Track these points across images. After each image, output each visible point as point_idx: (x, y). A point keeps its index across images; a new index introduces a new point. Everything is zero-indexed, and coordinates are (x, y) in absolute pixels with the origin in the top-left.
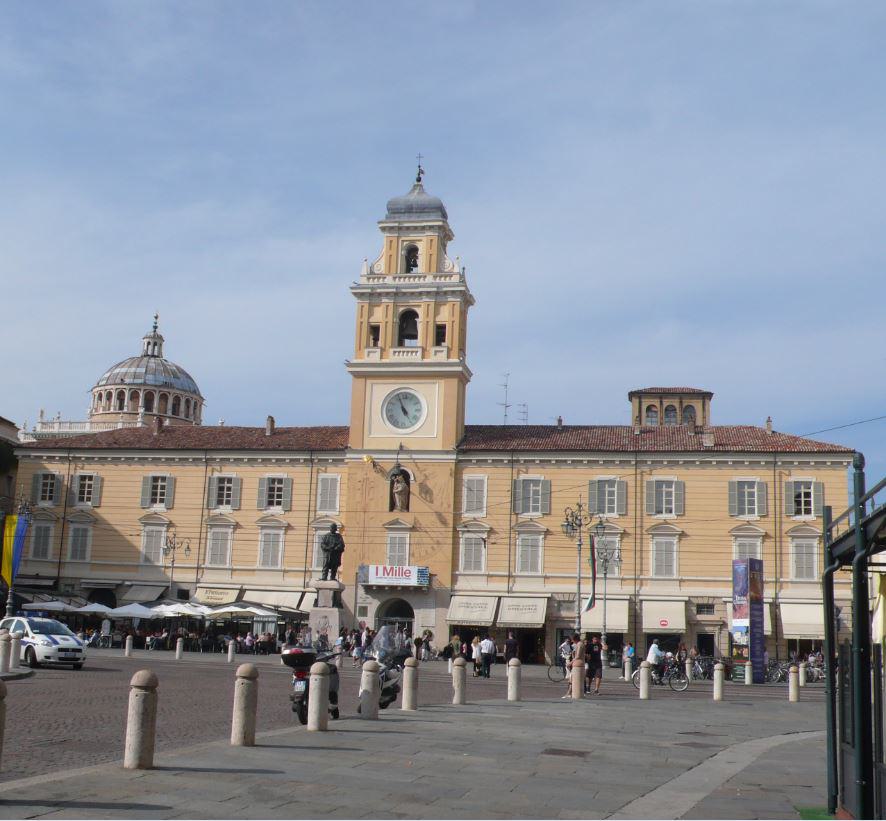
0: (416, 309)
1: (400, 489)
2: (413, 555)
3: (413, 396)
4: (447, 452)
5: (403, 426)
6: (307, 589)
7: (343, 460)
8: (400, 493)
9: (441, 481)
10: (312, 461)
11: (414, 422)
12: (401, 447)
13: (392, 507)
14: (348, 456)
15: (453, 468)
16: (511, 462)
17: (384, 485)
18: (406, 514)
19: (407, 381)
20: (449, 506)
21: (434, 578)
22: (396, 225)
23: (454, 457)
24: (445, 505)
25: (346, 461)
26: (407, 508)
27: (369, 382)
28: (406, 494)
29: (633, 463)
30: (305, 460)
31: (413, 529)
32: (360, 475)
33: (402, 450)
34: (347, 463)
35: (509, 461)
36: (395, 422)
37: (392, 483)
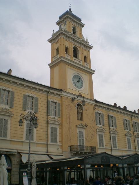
0: (78, 48)
6: (48, 154)
7: (59, 95)
10: (48, 92)
14: (63, 93)
16: (108, 109)
22: (72, 18)
23: (94, 103)
25: (61, 95)
27: (67, 66)
29: (131, 115)
30: (45, 91)
33: (80, 96)
34: (62, 97)
35: (107, 108)
37: (77, 109)
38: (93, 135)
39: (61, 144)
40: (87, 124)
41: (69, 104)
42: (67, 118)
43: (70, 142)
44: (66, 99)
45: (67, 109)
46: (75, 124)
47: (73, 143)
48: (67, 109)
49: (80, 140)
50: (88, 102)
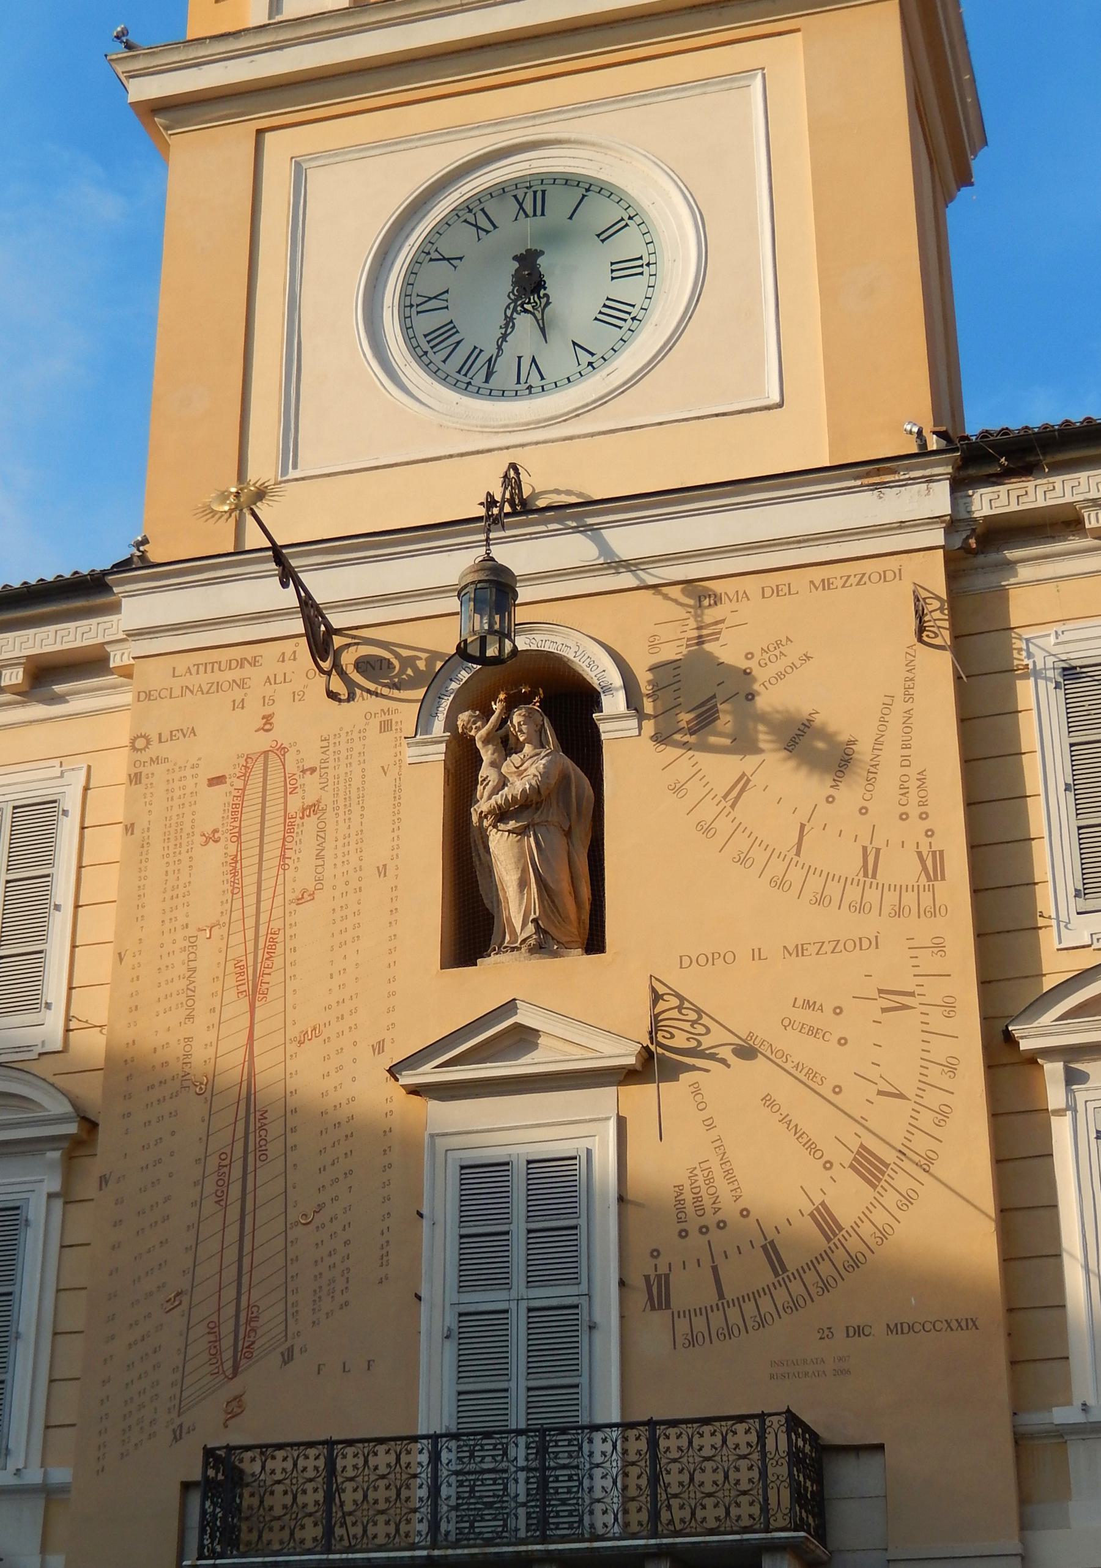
1: (518, 786)
2: (659, 1293)
3: (587, 189)
4: (875, 471)
5: (529, 381)
8: (520, 812)
9: (860, 656)
11: (600, 337)
12: (512, 478)
13: (471, 931)
14: (139, 608)
15: (937, 582)
17: (390, 777)
18: (577, 963)
19: (524, 139)
20: (933, 868)
21: (851, 1478)
24: (901, 868)
25: (118, 658)
26: (595, 943)
28: (573, 817)
31: (651, 1066)
32: (224, 735)
34: (127, 672)
36: (472, 371)
38: (868, 1167)
39: (61, 1475)
40: (675, 979)
41: (263, 742)
42: (190, 992)
43: (235, 1408)
44: (204, 679)
45: (212, 837)
46: (379, 1048)
47: (279, 1408)
48: (212, 837)
49: (476, 1335)
50: (902, 526)
